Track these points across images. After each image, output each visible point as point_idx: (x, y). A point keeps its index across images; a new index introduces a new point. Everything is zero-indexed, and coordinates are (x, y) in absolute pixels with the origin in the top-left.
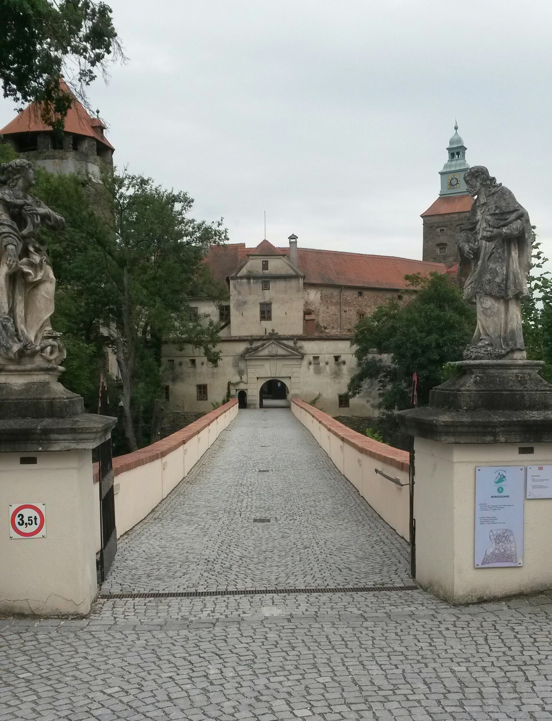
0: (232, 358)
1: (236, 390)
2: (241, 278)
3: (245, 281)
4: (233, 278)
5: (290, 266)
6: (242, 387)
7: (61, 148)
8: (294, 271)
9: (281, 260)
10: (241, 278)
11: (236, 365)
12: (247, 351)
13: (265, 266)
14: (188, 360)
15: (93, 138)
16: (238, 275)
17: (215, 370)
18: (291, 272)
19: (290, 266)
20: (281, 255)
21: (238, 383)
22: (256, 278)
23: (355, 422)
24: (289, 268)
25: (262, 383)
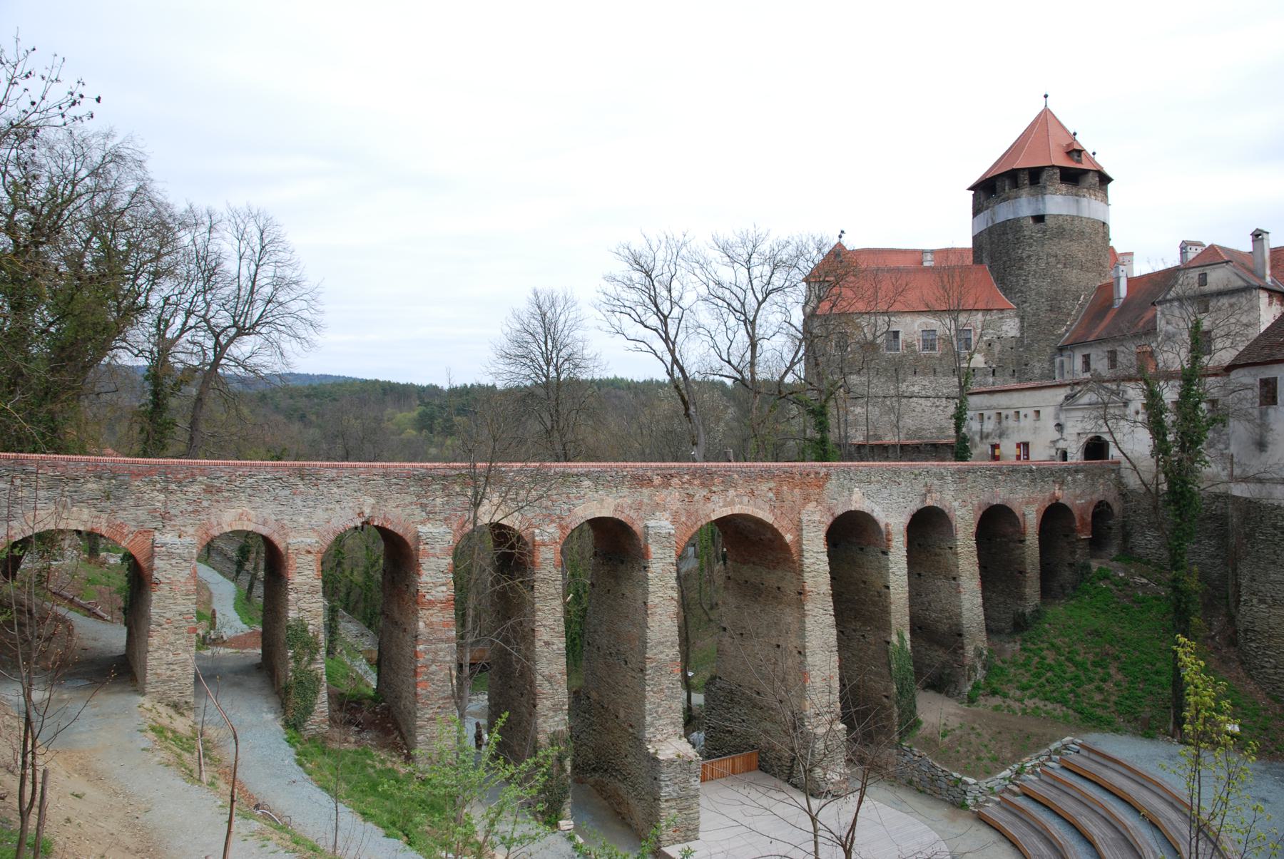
0: (1053, 408)
1: (1058, 449)
2: (1171, 301)
3: (1176, 304)
4: (1160, 303)
5: (1237, 274)
6: (1061, 445)
7: (1017, 187)
8: (1244, 280)
9: (1224, 269)
10: (1171, 301)
11: (1057, 417)
12: (1067, 398)
13: (1203, 280)
14: (1012, 412)
15: (1053, 166)
16: (1168, 297)
17: (1038, 424)
18: (1240, 283)
19: (1237, 274)
20: (1223, 263)
21: (1058, 440)
22: (1189, 298)
23: (1203, 499)
24: (1235, 277)
25: (1083, 440)
